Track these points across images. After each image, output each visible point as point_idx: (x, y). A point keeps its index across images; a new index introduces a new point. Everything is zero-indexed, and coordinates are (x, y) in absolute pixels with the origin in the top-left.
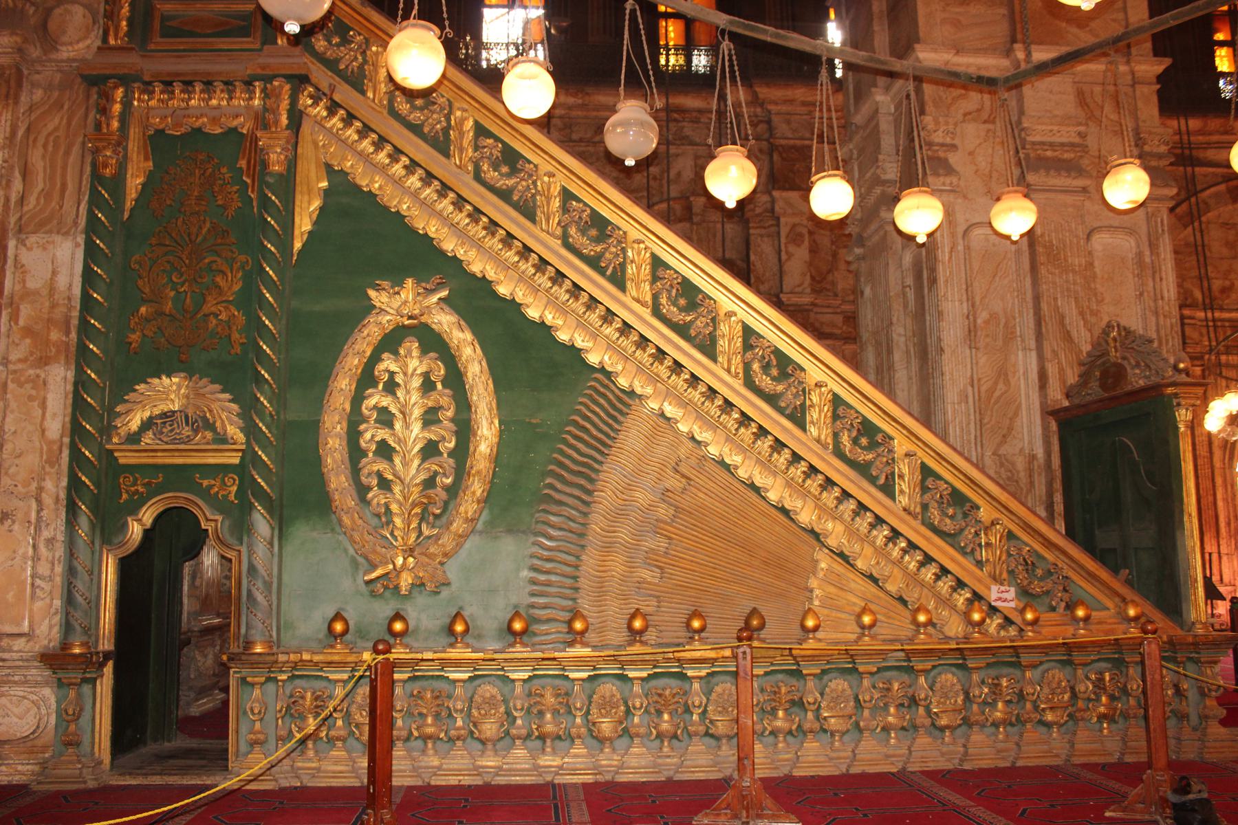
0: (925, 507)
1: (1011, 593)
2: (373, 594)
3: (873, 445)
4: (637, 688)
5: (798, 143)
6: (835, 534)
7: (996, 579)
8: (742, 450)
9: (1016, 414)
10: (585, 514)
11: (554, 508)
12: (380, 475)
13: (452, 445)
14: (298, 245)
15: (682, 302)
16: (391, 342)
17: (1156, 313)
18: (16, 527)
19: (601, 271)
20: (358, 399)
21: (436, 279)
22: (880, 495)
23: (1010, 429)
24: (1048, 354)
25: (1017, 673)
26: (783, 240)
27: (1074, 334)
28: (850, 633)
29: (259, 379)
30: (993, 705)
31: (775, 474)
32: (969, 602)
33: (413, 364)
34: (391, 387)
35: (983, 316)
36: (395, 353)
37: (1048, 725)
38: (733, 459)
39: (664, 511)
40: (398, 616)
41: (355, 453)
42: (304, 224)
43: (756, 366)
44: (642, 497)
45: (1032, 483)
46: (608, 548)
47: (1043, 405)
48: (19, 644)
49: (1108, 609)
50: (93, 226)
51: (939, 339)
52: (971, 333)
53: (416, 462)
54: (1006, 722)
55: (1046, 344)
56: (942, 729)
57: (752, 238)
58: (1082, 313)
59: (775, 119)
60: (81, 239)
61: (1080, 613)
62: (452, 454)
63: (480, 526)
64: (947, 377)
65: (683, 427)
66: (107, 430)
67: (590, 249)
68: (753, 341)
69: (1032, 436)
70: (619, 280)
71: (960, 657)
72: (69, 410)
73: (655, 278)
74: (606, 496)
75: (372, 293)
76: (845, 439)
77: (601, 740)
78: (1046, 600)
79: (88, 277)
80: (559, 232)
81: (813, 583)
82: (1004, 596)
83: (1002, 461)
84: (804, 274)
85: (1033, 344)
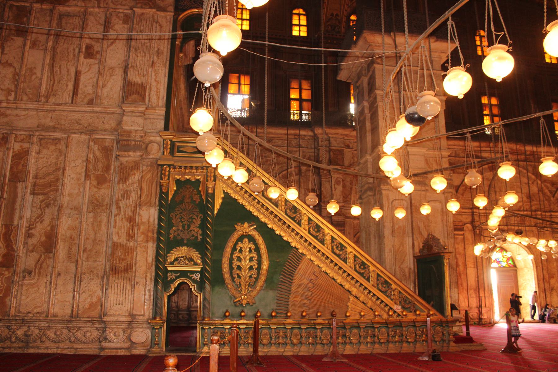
0: (378, 284)
1: (400, 307)
2: (236, 306)
3: (364, 268)
4: (303, 331)
5: (339, 148)
6: (354, 291)
7: (396, 303)
8: (331, 269)
9: (406, 256)
10: (291, 285)
11: (283, 284)
12: (238, 274)
13: (257, 267)
14: (216, 212)
15: (316, 230)
16: (241, 239)
17: (447, 227)
18: (140, 286)
19: (295, 221)
20: (232, 254)
21: (253, 223)
22: (366, 281)
23: (404, 260)
24: (415, 238)
25: (401, 329)
26: (333, 183)
27: (423, 232)
28: (358, 317)
29: (207, 248)
30: (395, 337)
31: (339, 275)
32: (389, 310)
33: (246, 245)
34: (241, 251)
35: (396, 227)
36: (242, 242)
37: (409, 342)
38: (329, 271)
39: (311, 285)
40: (243, 311)
41: (231, 268)
42: (217, 207)
43: (335, 247)
44: (305, 281)
45: (410, 276)
46: (296, 294)
47: (413, 254)
48: (141, 317)
49: (426, 313)
50: (161, 205)
51: (384, 234)
52: (393, 232)
53: (247, 271)
54: (398, 342)
55: (414, 236)
56: (382, 343)
57: (322, 182)
58: (425, 226)
59: (331, 139)
60: (157, 208)
61: (418, 313)
62: (256, 269)
63: (263, 288)
64: (386, 245)
65: (316, 263)
66: (165, 261)
67: (293, 215)
68: (334, 240)
69: (410, 263)
70: (299, 224)
71: (386, 324)
72: (154, 255)
73: (309, 223)
74: (296, 281)
75: (236, 226)
76: (357, 266)
77: (294, 345)
78: (409, 309)
79: (160, 220)
80: (284, 210)
81: (349, 304)
82: (398, 308)
83: (402, 270)
84: (340, 195)
85: (411, 235)
